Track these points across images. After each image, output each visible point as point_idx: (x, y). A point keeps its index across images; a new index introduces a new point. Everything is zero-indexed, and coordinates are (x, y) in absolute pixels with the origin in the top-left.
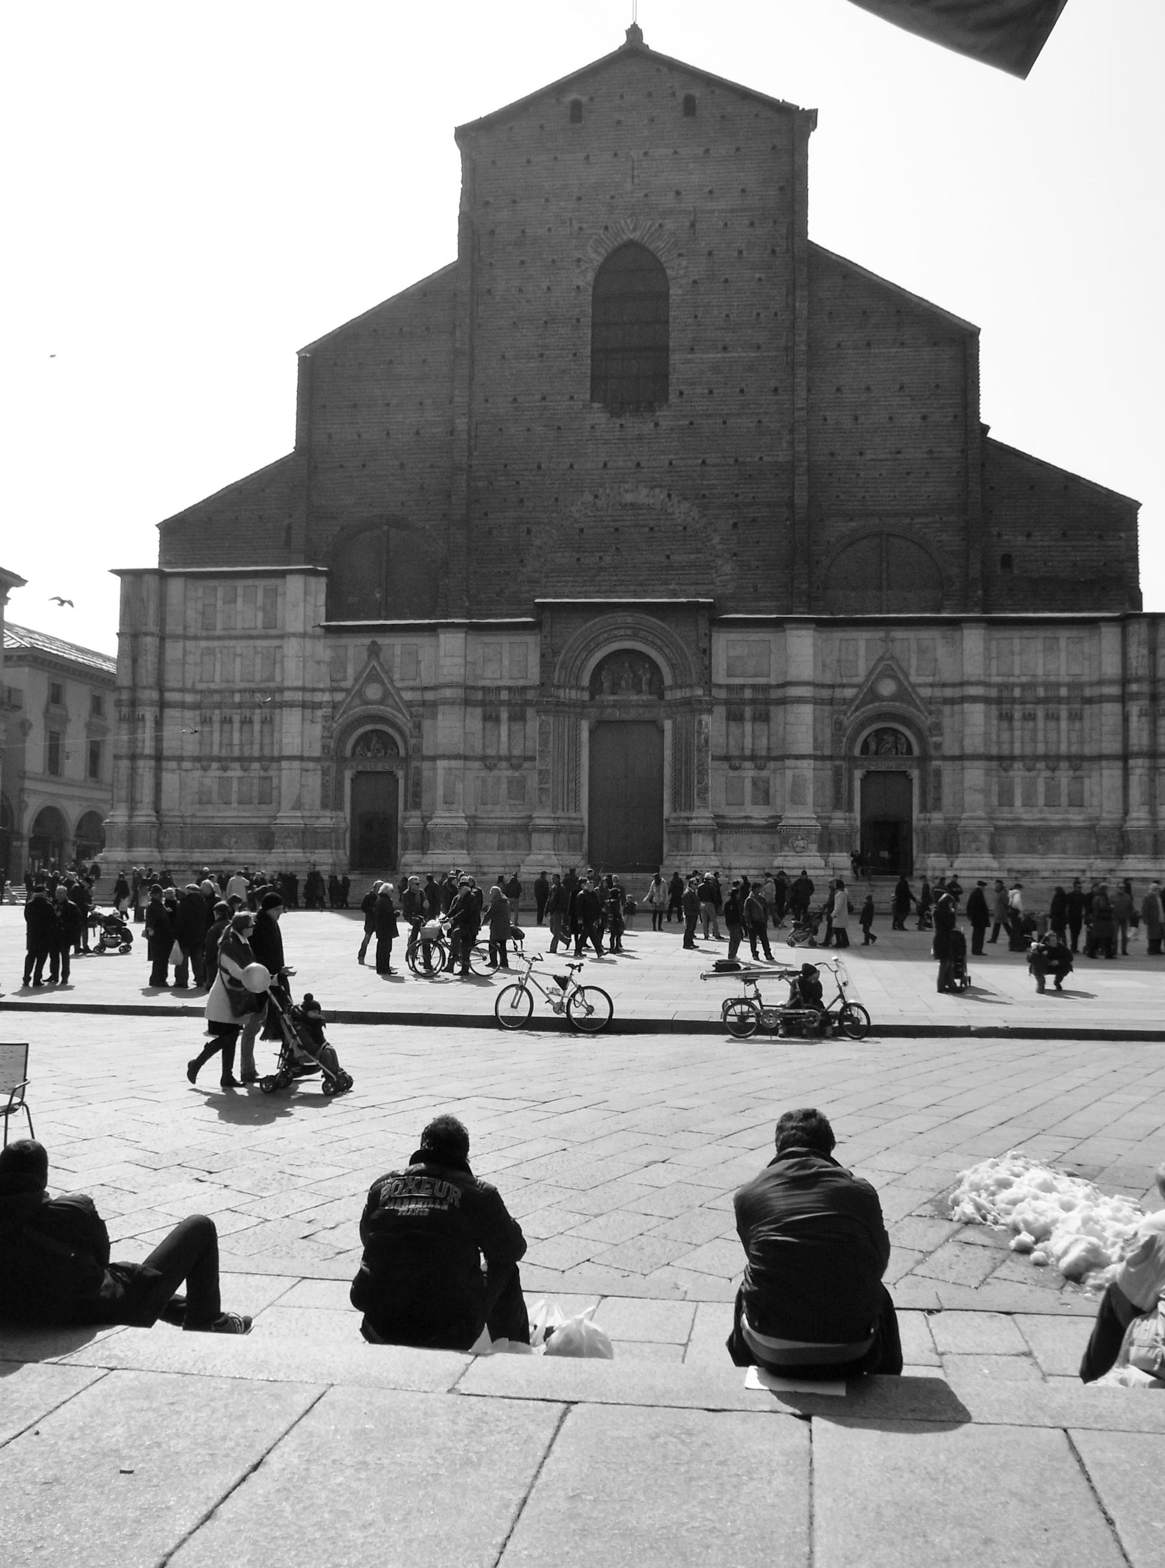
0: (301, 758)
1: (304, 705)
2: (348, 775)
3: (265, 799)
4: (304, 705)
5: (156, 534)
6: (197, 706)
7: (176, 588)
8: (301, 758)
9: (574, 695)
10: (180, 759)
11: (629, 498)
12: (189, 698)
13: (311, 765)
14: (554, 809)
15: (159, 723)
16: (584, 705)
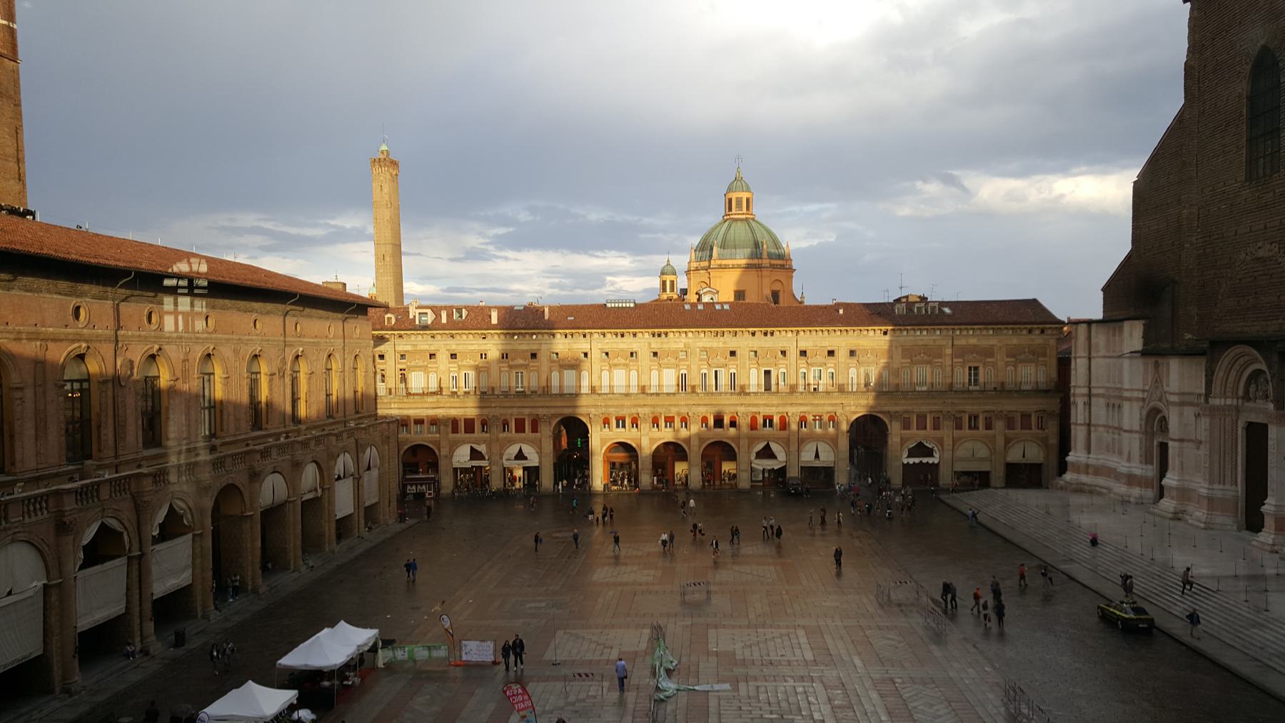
0: (1130, 431)
1: (1129, 399)
2: (1155, 443)
3: (1120, 453)
4: (1129, 399)
5: (1100, 296)
6: (1103, 396)
7: (1094, 326)
8: (1130, 431)
9: (1229, 402)
10: (1097, 426)
11: (1261, 253)
12: (1101, 391)
13: (1137, 436)
14: (1211, 482)
15: (1089, 405)
16: (1238, 409)
